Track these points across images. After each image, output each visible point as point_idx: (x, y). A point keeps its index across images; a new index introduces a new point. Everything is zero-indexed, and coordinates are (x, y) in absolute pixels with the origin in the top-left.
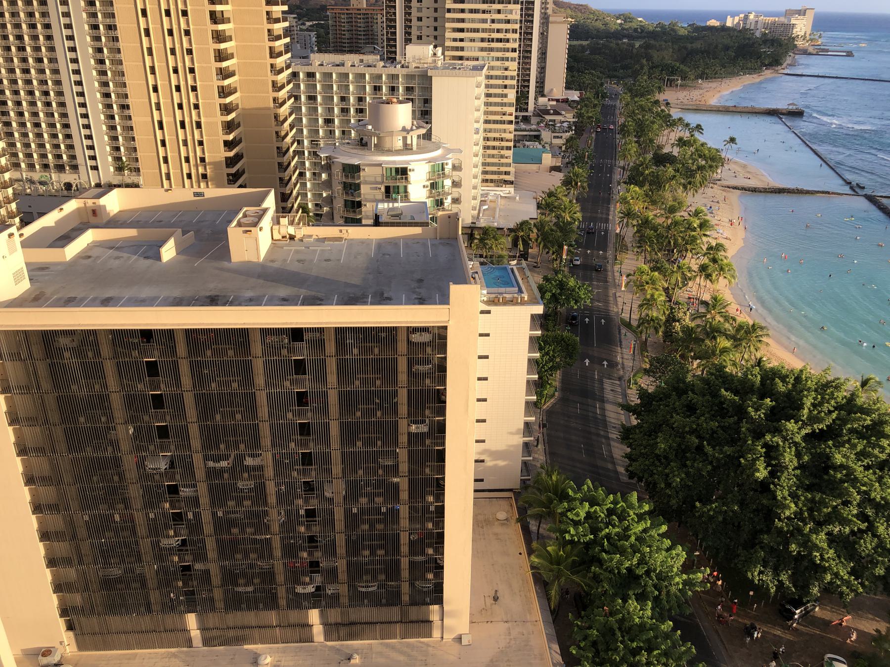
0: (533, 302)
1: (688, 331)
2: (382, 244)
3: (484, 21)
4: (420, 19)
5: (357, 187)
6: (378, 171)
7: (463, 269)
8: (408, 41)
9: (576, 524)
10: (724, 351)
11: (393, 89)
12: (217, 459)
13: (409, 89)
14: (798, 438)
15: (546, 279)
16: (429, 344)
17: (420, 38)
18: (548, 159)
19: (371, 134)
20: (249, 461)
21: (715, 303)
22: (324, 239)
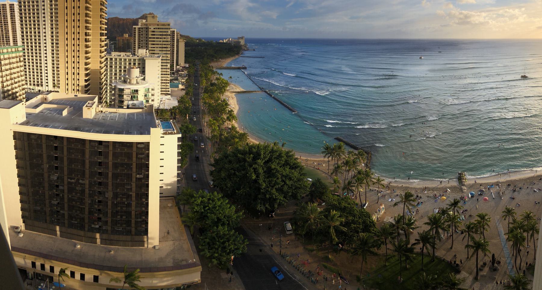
0: (178, 133)
1: (226, 138)
2: (129, 114)
3: (160, 41)
5: (123, 96)
6: (129, 91)
7: (155, 122)
9: (197, 205)
10: (237, 142)
11: (134, 64)
12: (71, 179)
13: (139, 64)
14: (262, 164)
15: (182, 126)
16: (144, 148)
18: (181, 87)
19: (128, 79)
21: (233, 128)
22: (111, 113)
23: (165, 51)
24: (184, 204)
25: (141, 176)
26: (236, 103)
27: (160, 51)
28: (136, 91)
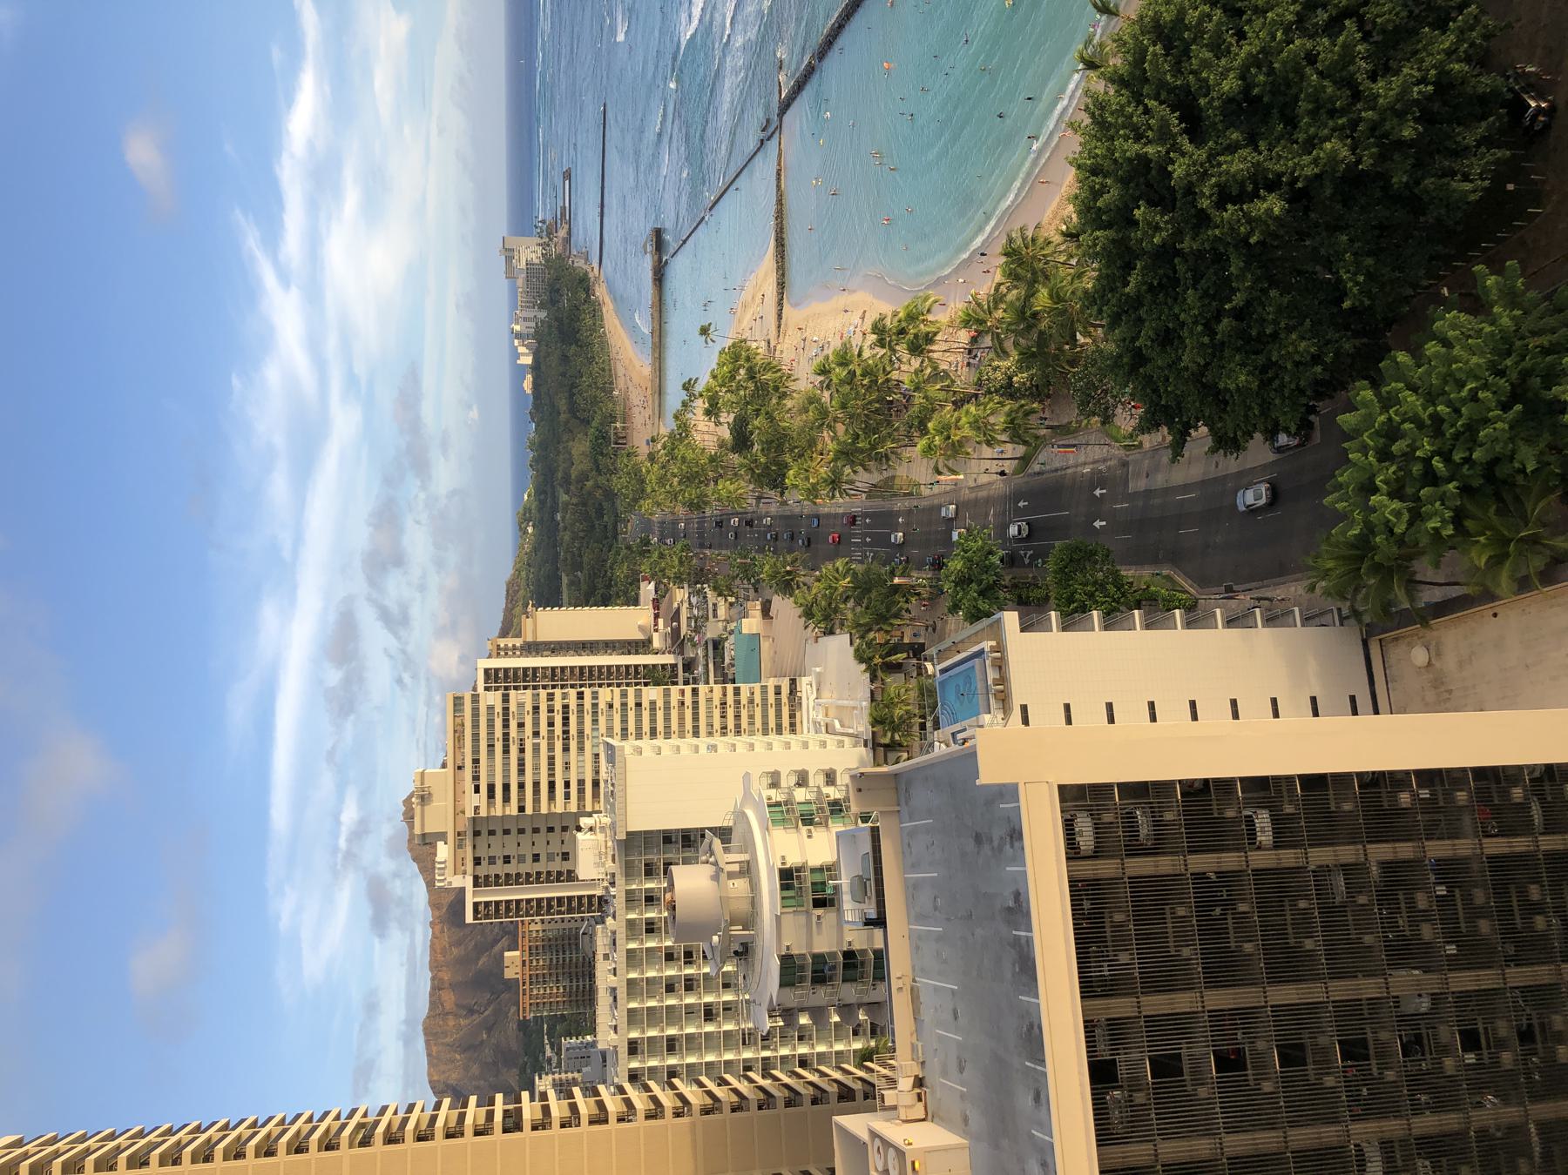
0: (997, 631)
1: (1027, 358)
3: (536, 748)
4: (536, 858)
5: (819, 958)
7: (949, 760)
8: (571, 876)
9: (1416, 516)
10: (1056, 297)
11: (650, 899)
13: (649, 872)
14: (1201, 154)
15: (954, 608)
17: (565, 857)
18: (752, 623)
19: (727, 939)
21: (974, 320)
23: (581, 722)
24: (1412, 584)
25: (1263, 820)
26: (843, 300)
27: (581, 749)
28: (788, 877)
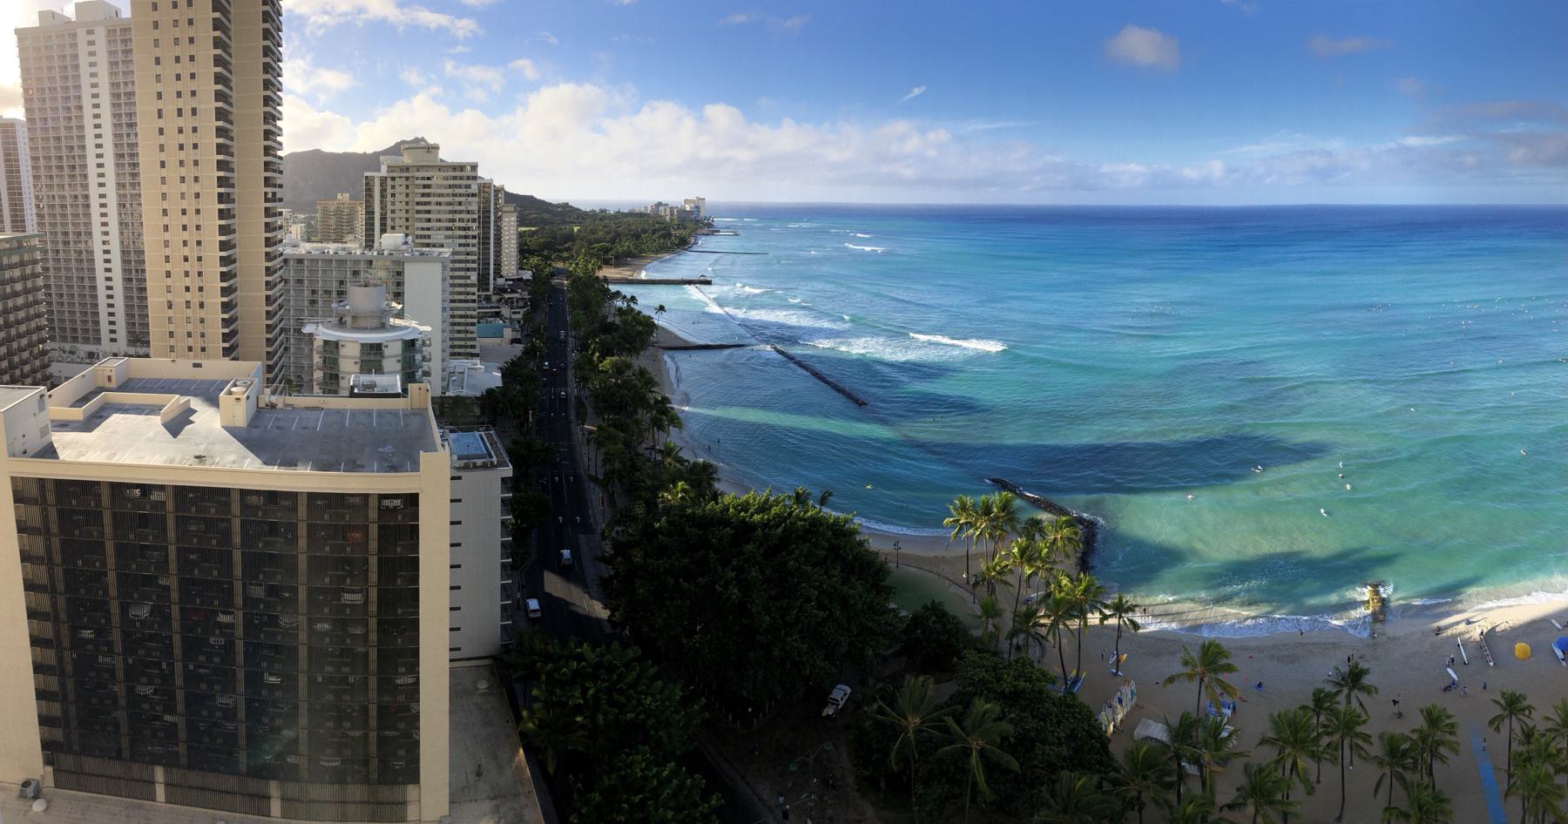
4: (393, 212)
8: (383, 231)
15: (515, 442)
17: (393, 228)
20: (222, 618)
